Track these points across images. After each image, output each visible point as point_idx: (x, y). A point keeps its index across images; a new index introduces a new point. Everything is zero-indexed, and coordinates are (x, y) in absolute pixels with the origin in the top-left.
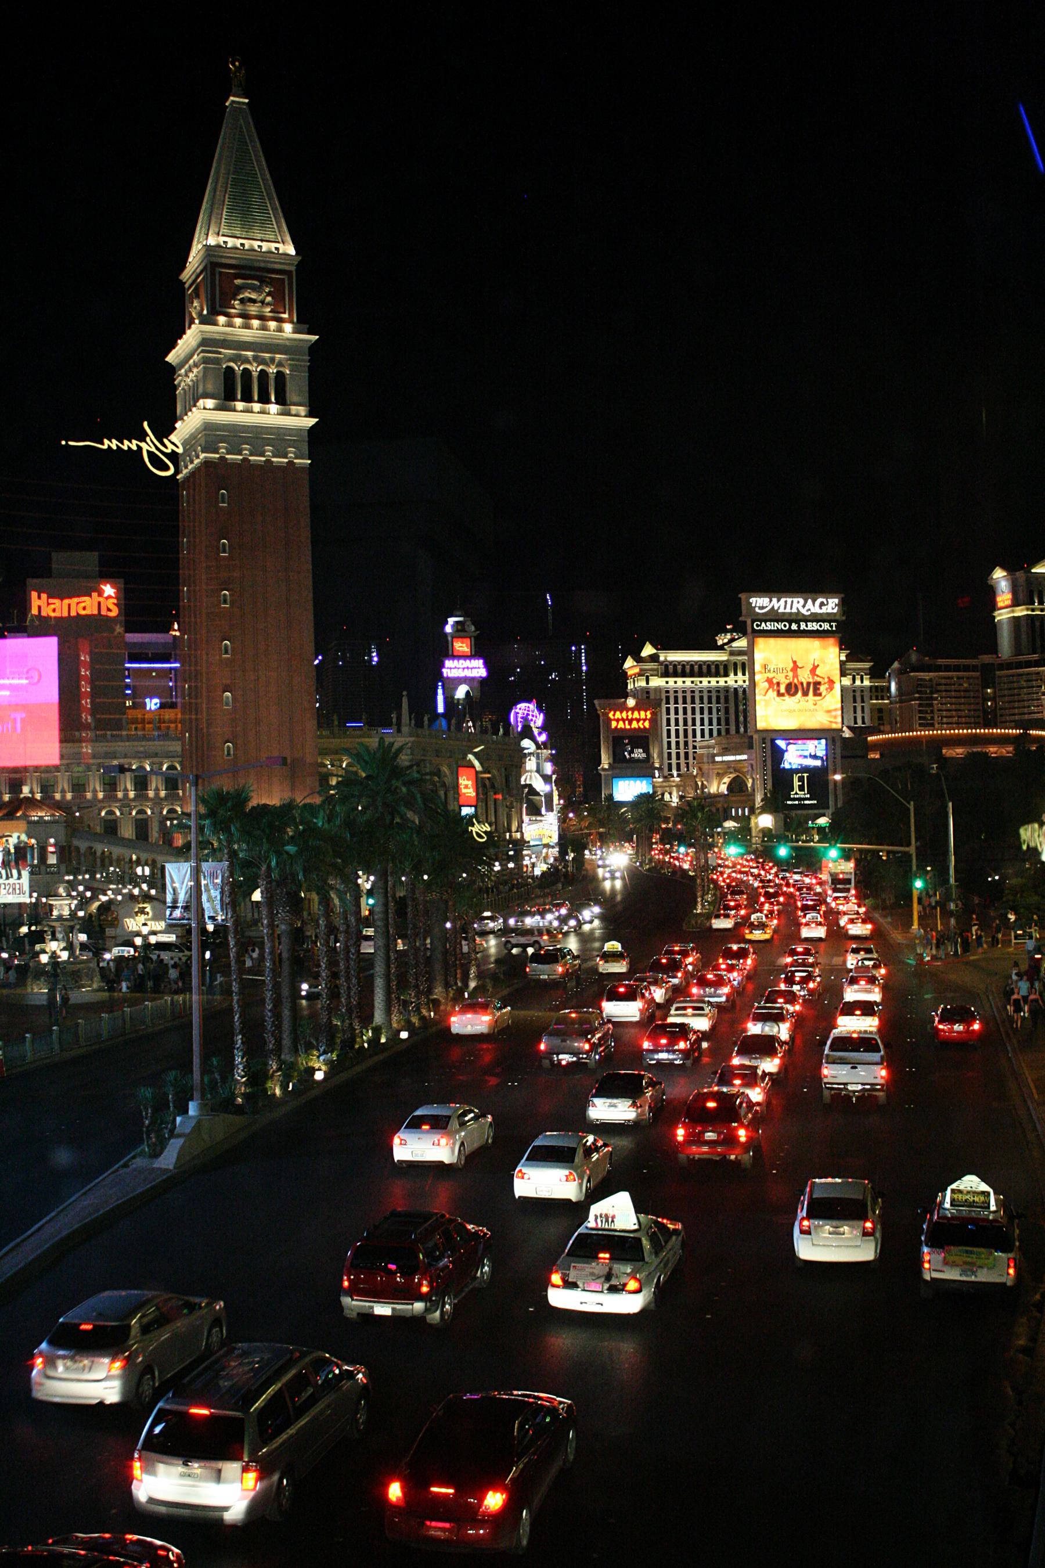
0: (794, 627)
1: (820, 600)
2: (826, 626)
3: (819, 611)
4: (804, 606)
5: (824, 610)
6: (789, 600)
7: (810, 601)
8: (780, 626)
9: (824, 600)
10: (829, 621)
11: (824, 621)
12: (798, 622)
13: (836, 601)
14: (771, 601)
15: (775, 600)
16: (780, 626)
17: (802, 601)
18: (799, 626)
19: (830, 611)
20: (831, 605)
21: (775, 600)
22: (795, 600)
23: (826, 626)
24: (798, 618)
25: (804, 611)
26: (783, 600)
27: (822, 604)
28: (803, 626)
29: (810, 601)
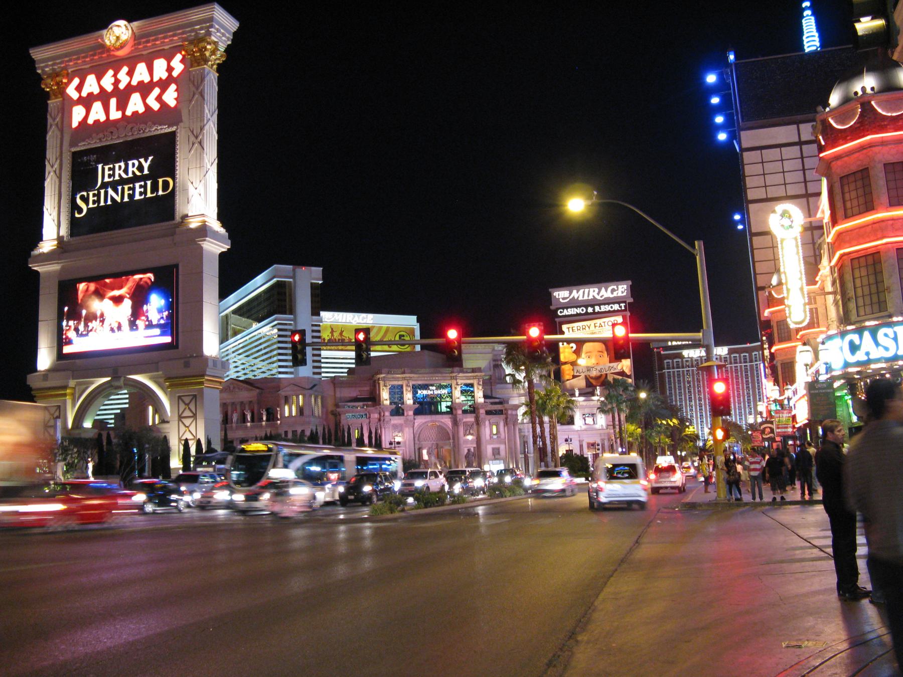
0: (590, 310)
1: (610, 289)
2: (616, 307)
3: (611, 296)
4: (598, 294)
5: (615, 294)
6: (587, 290)
7: (603, 289)
8: (579, 311)
9: (615, 287)
10: (619, 303)
11: (614, 303)
12: (593, 306)
13: (625, 286)
14: (570, 294)
15: (575, 292)
16: (579, 311)
17: (597, 290)
18: (594, 310)
19: (620, 294)
20: (621, 290)
21: (575, 292)
22: (591, 290)
23: (616, 307)
24: (593, 303)
25: (598, 297)
26: (582, 291)
27: (613, 291)
28: (597, 309)
29: (603, 289)
